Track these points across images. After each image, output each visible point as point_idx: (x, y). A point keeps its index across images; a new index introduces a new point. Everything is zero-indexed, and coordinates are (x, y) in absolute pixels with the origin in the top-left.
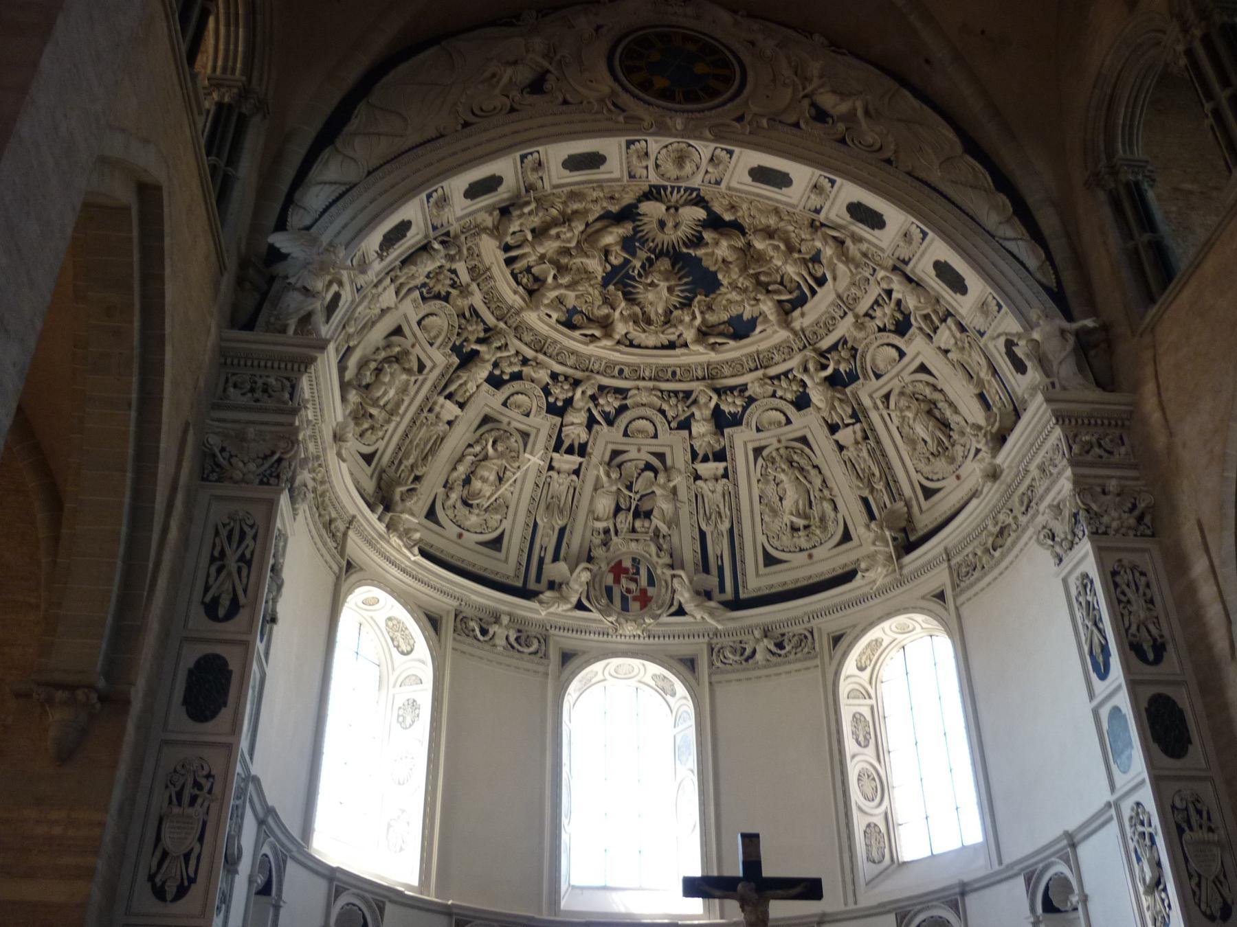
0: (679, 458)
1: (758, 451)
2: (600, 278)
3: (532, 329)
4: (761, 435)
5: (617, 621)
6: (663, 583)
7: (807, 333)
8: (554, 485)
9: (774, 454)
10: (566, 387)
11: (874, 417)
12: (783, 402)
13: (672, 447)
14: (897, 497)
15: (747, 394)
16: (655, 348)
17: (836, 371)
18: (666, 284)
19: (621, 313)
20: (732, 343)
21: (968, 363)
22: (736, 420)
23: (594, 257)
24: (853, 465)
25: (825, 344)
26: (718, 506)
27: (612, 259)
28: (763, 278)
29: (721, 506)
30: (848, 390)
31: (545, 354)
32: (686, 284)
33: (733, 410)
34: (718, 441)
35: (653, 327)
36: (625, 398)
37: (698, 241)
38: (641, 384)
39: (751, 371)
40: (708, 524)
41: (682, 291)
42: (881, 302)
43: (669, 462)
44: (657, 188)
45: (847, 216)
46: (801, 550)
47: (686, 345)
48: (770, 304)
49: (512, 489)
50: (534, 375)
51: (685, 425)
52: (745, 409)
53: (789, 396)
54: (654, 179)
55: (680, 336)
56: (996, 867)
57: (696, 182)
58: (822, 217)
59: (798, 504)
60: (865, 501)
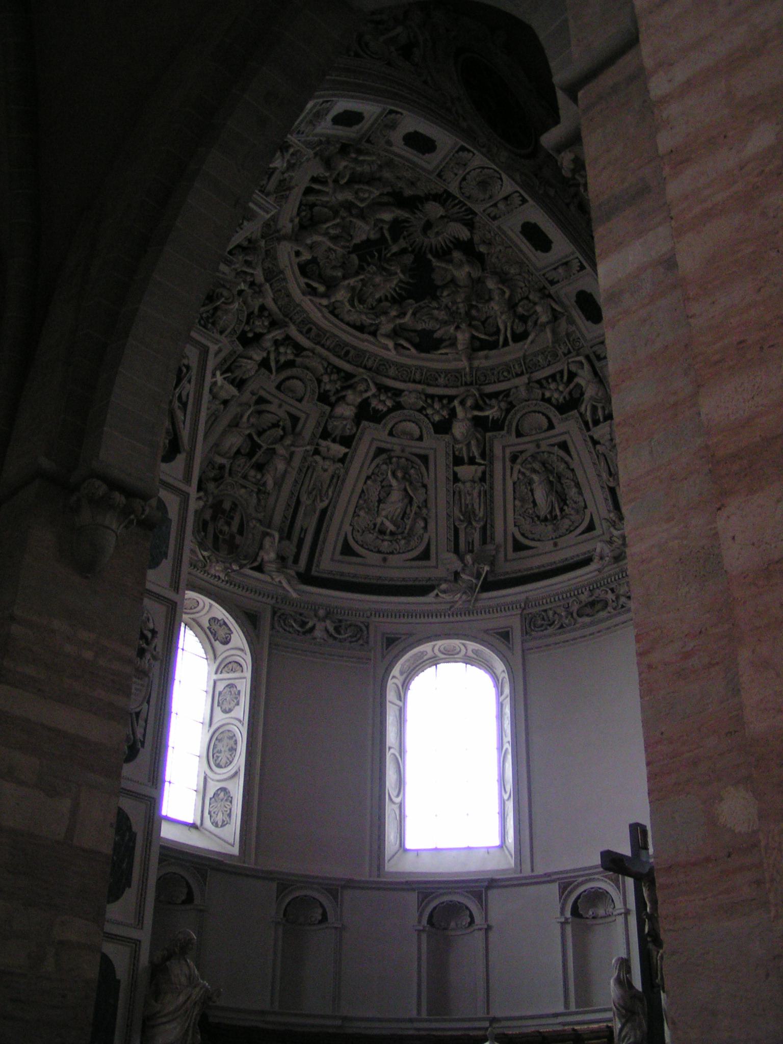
0: (309, 428)
1: (380, 451)
2: (352, 244)
3: (276, 259)
4: (390, 439)
5: (209, 558)
6: (250, 536)
7: (479, 373)
10: (266, 323)
11: (498, 466)
12: (426, 419)
14: (488, 540)
15: (398, 399)
16: (348, 324)
20: (413, 350)
22: (377, 417)
24: (460, 496)
25: (489, 389)
26: (321, 486)
29: (325, 486)
30: (489, 434)
31: (271, 285)
33: (380, 407)
35: (361, 306)
36: (297, 355)
37: (444, 254)
38: (319, 349)
39: (414, 381)
43: (298, 429)
44: (449, 195)
45: (574, 299)
46: (379, 552)
47: (374, 334)
48: (467, 335)
50: (249, 299)
52: (390, 410)
53: (437, 418)
54: (453, 188)
56: (527, 871)
57: (478, 208)
58: (552, 290)
60: (456, 531)
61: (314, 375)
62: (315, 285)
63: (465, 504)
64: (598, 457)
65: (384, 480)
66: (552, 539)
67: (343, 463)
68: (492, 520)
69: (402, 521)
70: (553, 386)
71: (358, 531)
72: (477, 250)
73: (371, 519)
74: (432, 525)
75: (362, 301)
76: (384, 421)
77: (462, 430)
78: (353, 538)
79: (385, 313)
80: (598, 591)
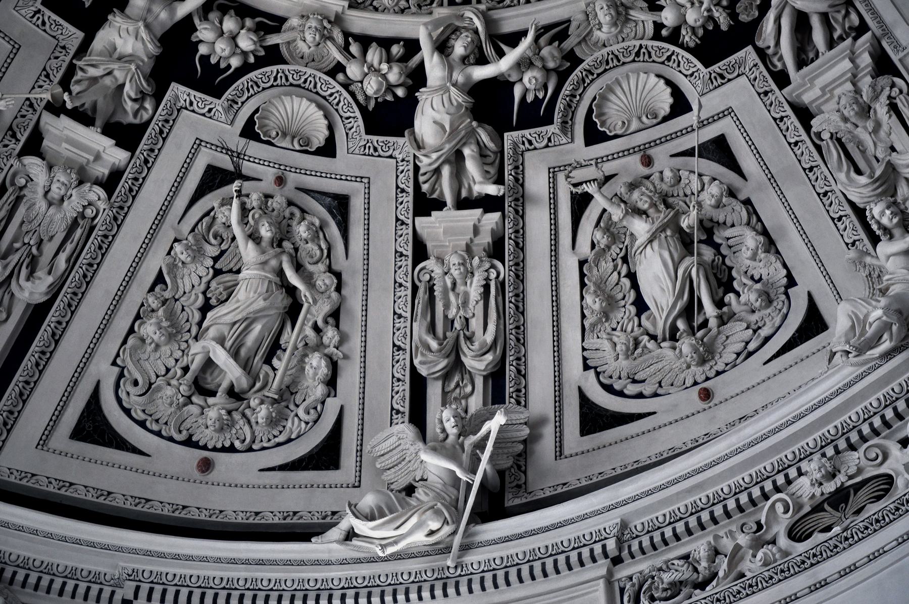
9: (254, 200)
12: (345, 94)
21: (859, 144)
26: (40, 243)
30: (510, 137)
33: (222, 48)
34: (140, 99)
46: (189, 443)
53: (372, 86)
59: (246, 330)
63: (446, 317)
64: (819, 148)
65: (223, 253)
66: (695, 383)
67: (110, 195)
68: (521, 360)
69: (266, 368)
71: (136, 383)
73: (178, 354)
74: (349, 379)
76: (229, 93)
77: (438, 117)
78: (119, 401)
80: (853, 459)
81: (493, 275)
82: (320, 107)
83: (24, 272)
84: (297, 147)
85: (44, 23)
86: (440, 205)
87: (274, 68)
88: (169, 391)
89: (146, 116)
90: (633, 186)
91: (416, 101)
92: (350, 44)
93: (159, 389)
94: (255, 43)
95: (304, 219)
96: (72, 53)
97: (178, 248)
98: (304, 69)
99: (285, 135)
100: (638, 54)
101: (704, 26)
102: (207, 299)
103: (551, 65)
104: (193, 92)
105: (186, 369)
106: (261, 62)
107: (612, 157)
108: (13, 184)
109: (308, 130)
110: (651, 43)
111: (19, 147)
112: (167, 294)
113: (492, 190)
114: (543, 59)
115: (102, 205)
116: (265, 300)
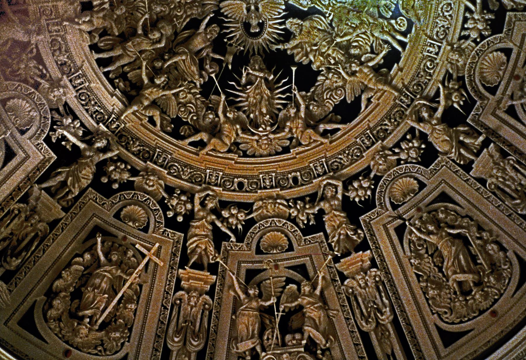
1: (400, 231)
2: (199, 86)
3: (138, 139)
8: (186, 308)
11: (506, 133)
13: (311, 257)
15: (372, 176)
16: (270, 155)
17: (449, 111)
18: (262, 75)
19: (225, 116)
23: (184, 53)
26: (374, 303)
27: (208, 67)
28: (353, 51)
29: (378, 301)
32: (285, 84)
35: (261, 129)
36: (251, 213)
39: (368, 148)
40: (367, 322)
41: (282, 93)
42: (467, 15)
43: (311, 273)
46: (481, 312)
47: (300, 144)
48: (366, 70)
49: (133, 306)
51: (320, 226)
52: (373, 191)
55: (291, 139)
59: (459, 261)
61: (283, 218)
62: (196, 138)
63: (512, 190)
65: (427, 248)
67: (377, 268)
69: (478, 266)
70: (469, 25)
71: (446, 313)
72: (306, 9)
73: (448, 291)
74: (505, 241)
75: (257, 127)
78: (447, 323)
79: (287, 118)
81: (512, 162)
82: (406, 177)
83: (379, 315)
84: (412, 195)
85: (310, 241)
86: (472, 162)
87: (381, 182)
88: (458, 304)
89: (362, 235)
90: (522, 89)
91: (431, 143)
92: (394, 151)
93: (454, 306)
94: (368, 181)
95: (438, 213)
96: (325, 241)
97: (412, 261)
98: (389, 173)
99: (405, 195)
100: (478, 54)
101: (487, 25)
102: (438, 267)
103: (456, 87)
104: (367, 214)
105: (455, 293)
106: (376, 185)
107: (506, 89)
108: (349, 294)
109: (411, 187)
110: (478, 48)
111: (339, 282)
112: (425, 278)
113: (481, 139)
114: (452, 88)
115: (379, 273)
116: (454, 246)
